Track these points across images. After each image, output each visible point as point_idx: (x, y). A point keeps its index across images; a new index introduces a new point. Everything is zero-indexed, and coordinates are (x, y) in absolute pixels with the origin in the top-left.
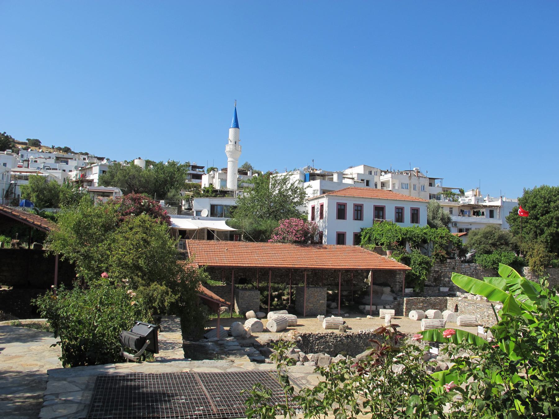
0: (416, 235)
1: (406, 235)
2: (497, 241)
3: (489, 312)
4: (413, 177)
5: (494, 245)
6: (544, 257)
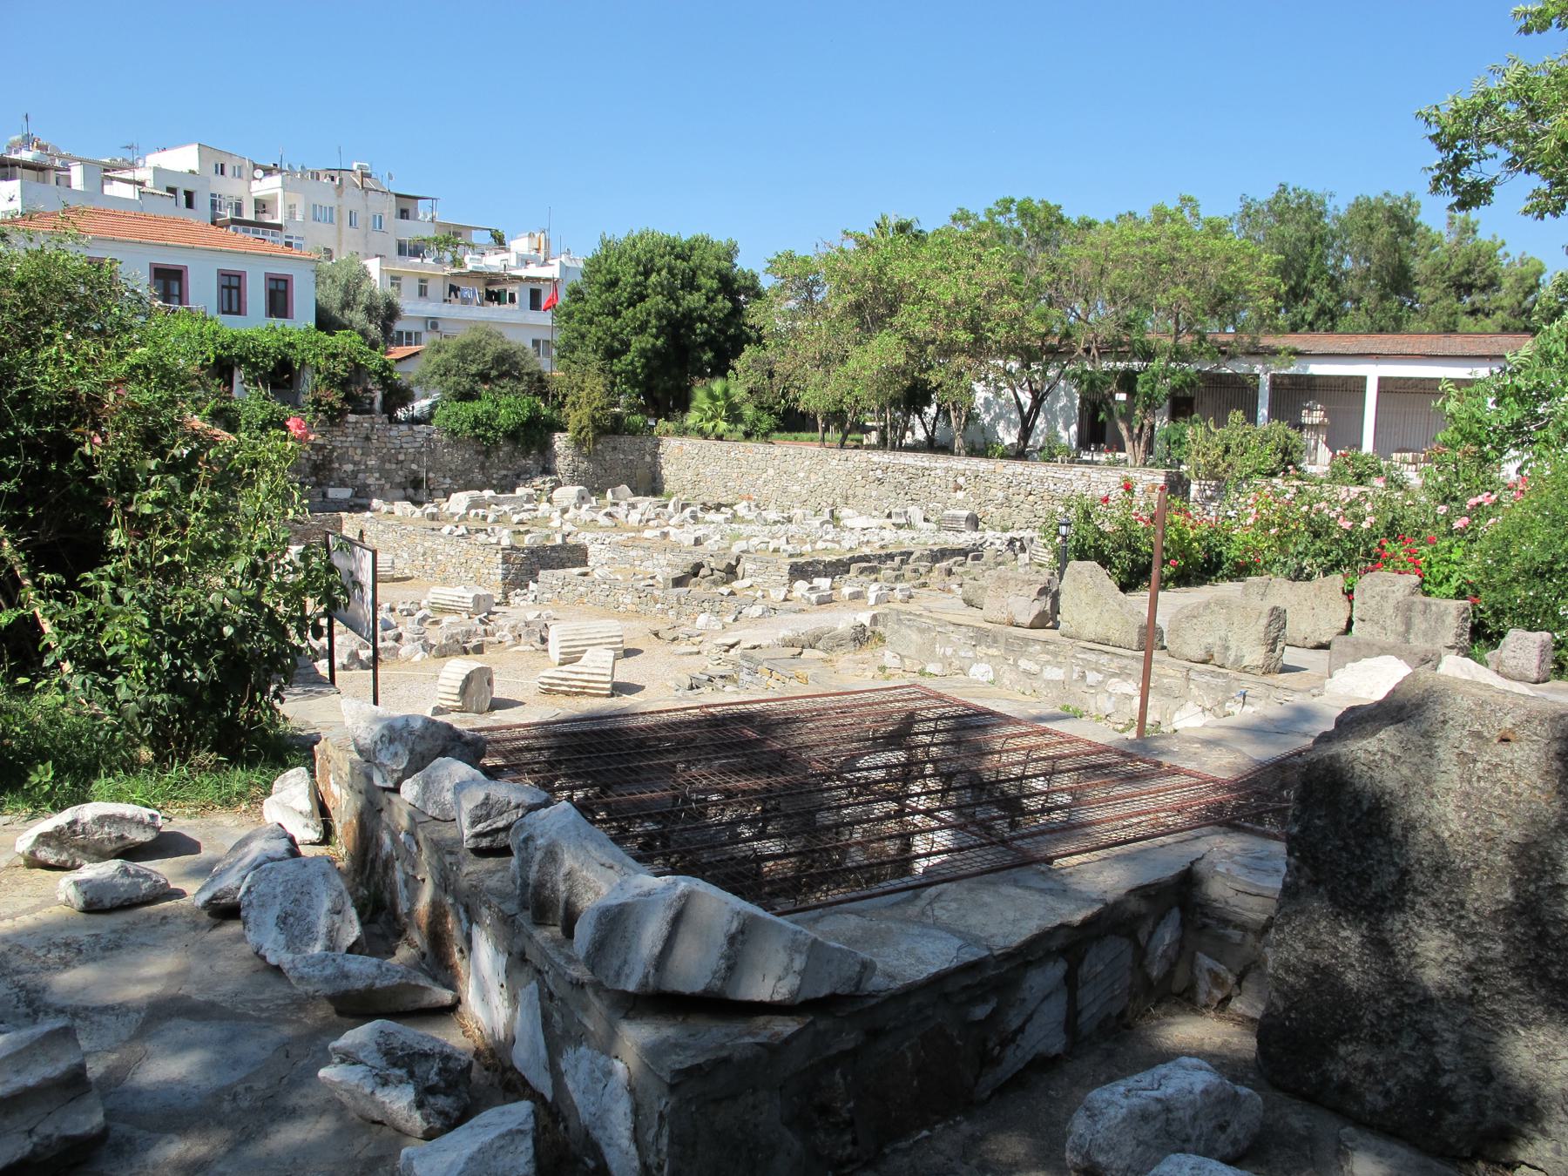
0: (260, 349)
1: (230, 347)
2: (491, 368)
3: (426, 544)
4: (348, 190)
5: (484, 377)
6: (603, 408)
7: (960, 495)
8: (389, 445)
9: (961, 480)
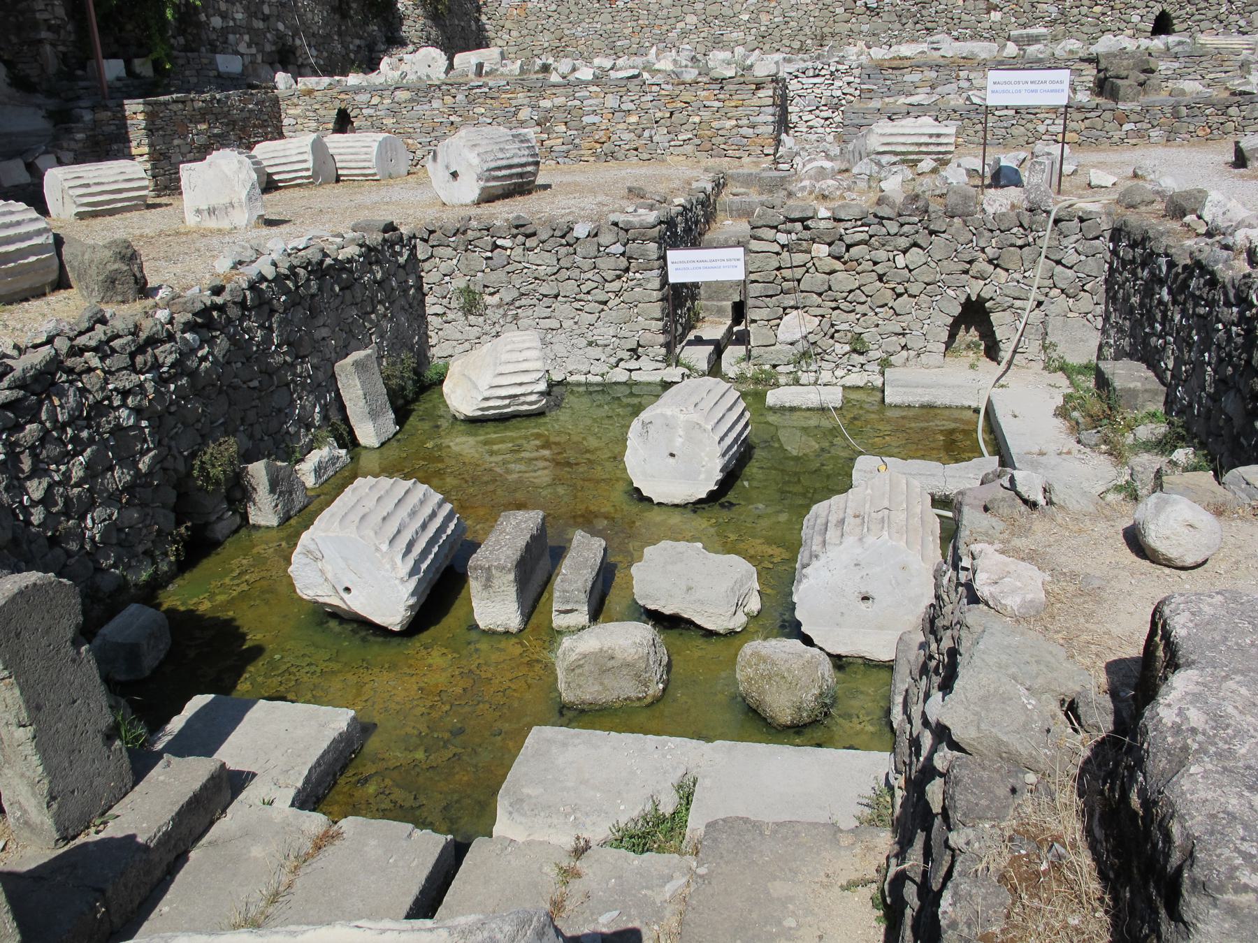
7: (996, 16)
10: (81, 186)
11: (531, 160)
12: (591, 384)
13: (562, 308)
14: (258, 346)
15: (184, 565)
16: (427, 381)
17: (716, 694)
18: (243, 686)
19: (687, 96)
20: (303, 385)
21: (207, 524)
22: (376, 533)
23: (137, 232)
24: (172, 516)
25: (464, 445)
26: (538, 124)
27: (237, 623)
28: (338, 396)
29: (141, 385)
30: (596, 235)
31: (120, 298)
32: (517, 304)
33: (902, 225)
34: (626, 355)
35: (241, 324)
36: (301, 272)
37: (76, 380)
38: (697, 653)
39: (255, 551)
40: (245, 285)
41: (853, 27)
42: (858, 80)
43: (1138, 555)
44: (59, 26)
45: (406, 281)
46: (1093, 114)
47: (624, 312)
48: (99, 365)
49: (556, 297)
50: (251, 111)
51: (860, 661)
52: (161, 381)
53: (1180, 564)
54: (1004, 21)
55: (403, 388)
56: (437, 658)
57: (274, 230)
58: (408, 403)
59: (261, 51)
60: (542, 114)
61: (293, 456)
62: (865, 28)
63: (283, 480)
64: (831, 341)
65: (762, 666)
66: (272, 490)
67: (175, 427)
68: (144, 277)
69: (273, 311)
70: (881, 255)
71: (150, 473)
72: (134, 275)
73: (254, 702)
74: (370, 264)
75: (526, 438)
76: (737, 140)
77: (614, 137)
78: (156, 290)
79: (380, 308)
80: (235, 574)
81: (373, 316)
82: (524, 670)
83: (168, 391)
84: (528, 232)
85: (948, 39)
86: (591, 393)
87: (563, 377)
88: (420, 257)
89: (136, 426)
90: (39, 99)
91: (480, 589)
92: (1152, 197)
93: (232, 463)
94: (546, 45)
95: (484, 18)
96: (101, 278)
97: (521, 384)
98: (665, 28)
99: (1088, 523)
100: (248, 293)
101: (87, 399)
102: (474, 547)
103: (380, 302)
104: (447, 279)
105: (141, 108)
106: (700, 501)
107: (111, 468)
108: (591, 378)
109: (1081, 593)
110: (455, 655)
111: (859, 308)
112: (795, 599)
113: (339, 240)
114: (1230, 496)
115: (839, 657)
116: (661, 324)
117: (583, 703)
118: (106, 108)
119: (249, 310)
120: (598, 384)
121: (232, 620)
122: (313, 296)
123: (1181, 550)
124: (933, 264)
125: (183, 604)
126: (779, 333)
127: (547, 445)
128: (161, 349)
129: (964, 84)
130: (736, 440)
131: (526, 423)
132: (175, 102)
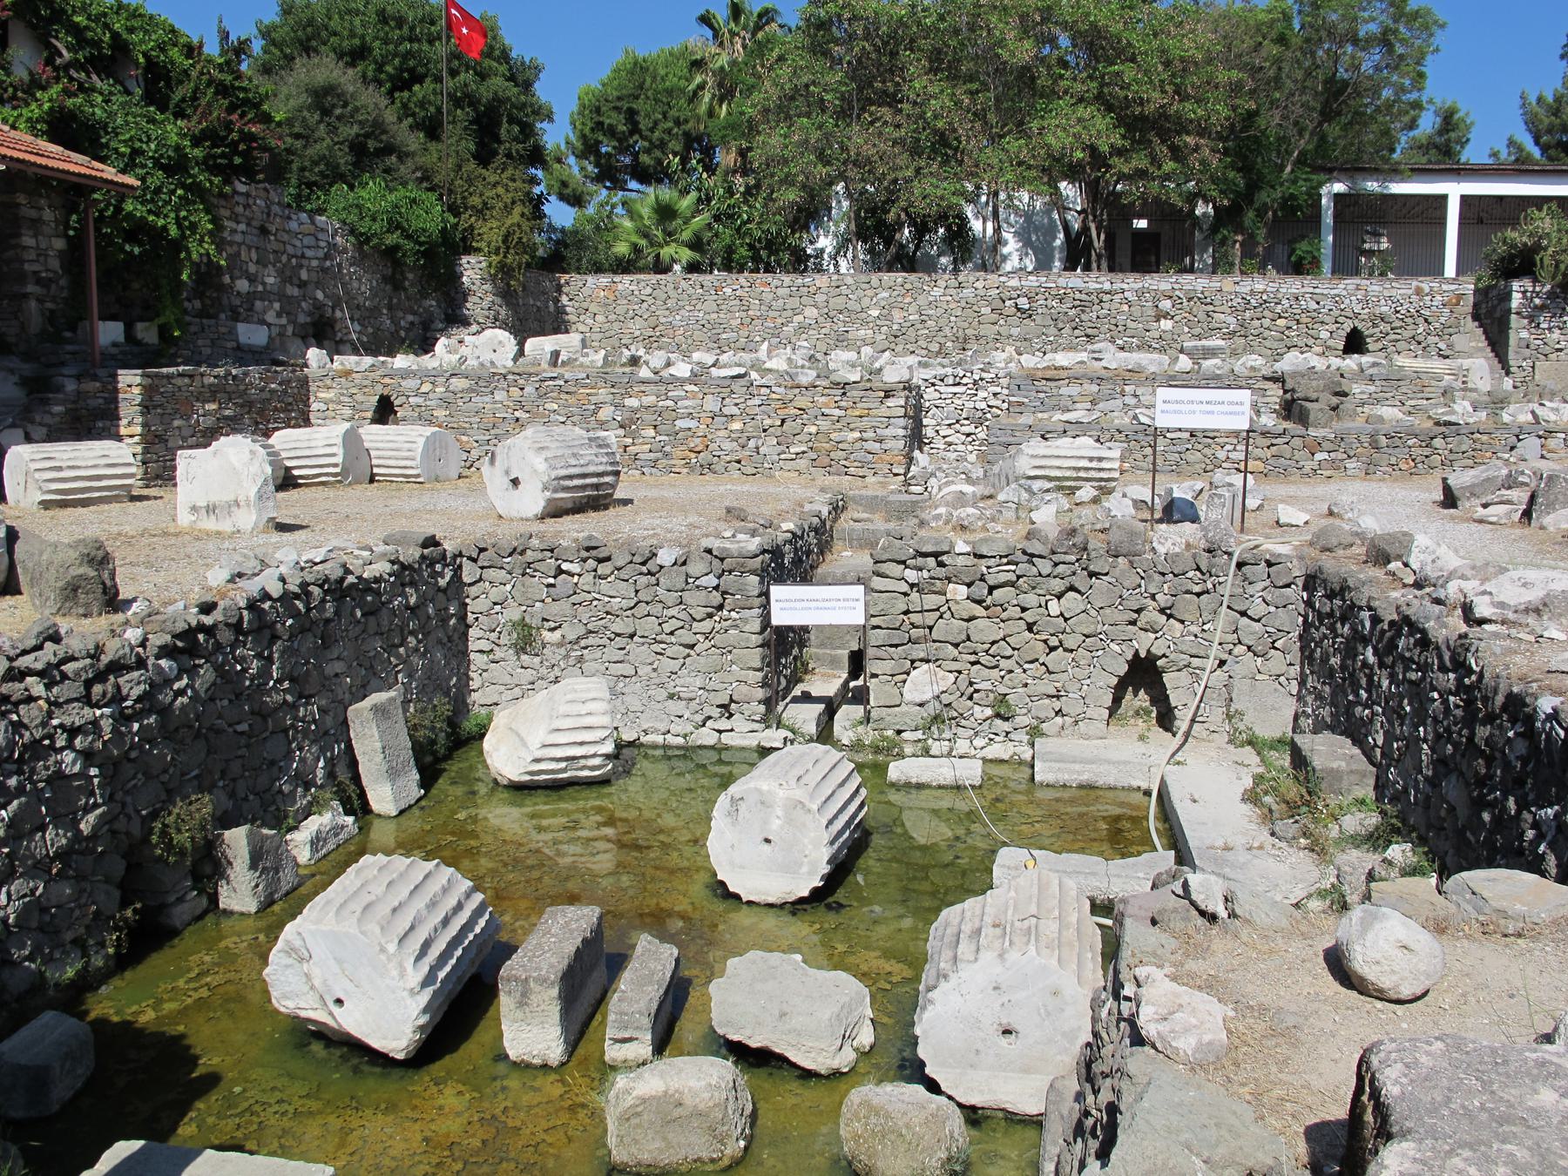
2: (367, 136)
3: (632, 402)
7: (1166, 324)
8: (290, 249)
9: (1166, 305)
10: (51, 469)
11: (610, 468)
12: (670, 747)
13: (639, 651)
14: (252, 680)
15: (124, 962)
16: (464, 735)
17: (813, 1157)
18: (187, 1130)
19: (802, 402)
20: (306, 733)
21: (163, 907)
22: (382, 928)
23: (115, 529)
24: (117, 894)
25: (505, 818)
26: (621, 427)
27: (187, 1042)
28: (350, 747)
29: (95, 723)
30: (684, 563)
31: (81, 611)
32: (583, 643)
33: (1056, 565)
34: (716, 712)
35: (233, 652)
36: (316, 590)
37: (10, 712)
38: (793, 1100)
39: (223, 944)
40: (243, 604)
41: (1002, 330)
42: (1006, 392)
43: (1342, 984)
44: (50, 280)
45: (447, 609)
46: (1279, 441)
47: (714, 658)
48: (44, 694)
49: (632, 636)
50: (273, 391)
51: (1000, 1114)
52: (122, 718)
53: (1394, 997)
54: (1176, 331)
55: (433, 742)
56: (450, 1097)
57: (287, 536)
58: (438, 760)
59: (293, 322)
60: (627, 415)
61: (283, 822)
62: (1015, 331)
63: (268, 852)
64: (970, 703)
65: (873, 1120)
66: (253, 866)
67: (134, 777)
68: (115, 586)
69: (275, 637)
70: (1030, 599)
71: (94, 836)
72: (103, 583)
73: (198, 1153)
74: (403, 585)
75: (584, 811)
76: (860, 455)
77: (712, 446)
78: (128, 603)
79: (412, 641)
80: (192, 975)
81: (402, 650)
82: (564, 1117)
83: (130, 732)
84: (601, 556)
85: (1112, 348)
86: (669, 758)
87: (635, 736)
88: (466, 579)
89: (83, 775)
90: (14, 362)
91: (512, 1006)
92: (1350, 539)
93: (203, 828)
94: (637, 333)
95: (564, 299)
96: (60, 584)
97: (582, 744)
98: (779, 321)
99: (1280, 941)
100: (245, 613)
101: (22, 736)
102: (509, 950)
103: (412, 633)
104: (498, 608)
105: (138, 380)
106: (802, 901)
107: (43, 828)
108: (671, 740)
109: (1273, 1033)
110: (476, 1095)
111: (1004, 664)
112: (918, 1031)
113: (366, 554)
114: (1453, 908)
115: (973, 1108)
116: (760, 675)
117: (639, 1164)
118: (95, 378)
119: (246, 634)
120: (678, 747)
121: (183, 1036)
122: (328, 621)
123: (1395, 978)
124: (1093, 612)
125: (117, 1013)
126: (905, 690)
127: (611, 822)
128: (127, 677)
129: (1131, 401)
130: (848, 824)
131: (586, 792)
132: (180, 375)
